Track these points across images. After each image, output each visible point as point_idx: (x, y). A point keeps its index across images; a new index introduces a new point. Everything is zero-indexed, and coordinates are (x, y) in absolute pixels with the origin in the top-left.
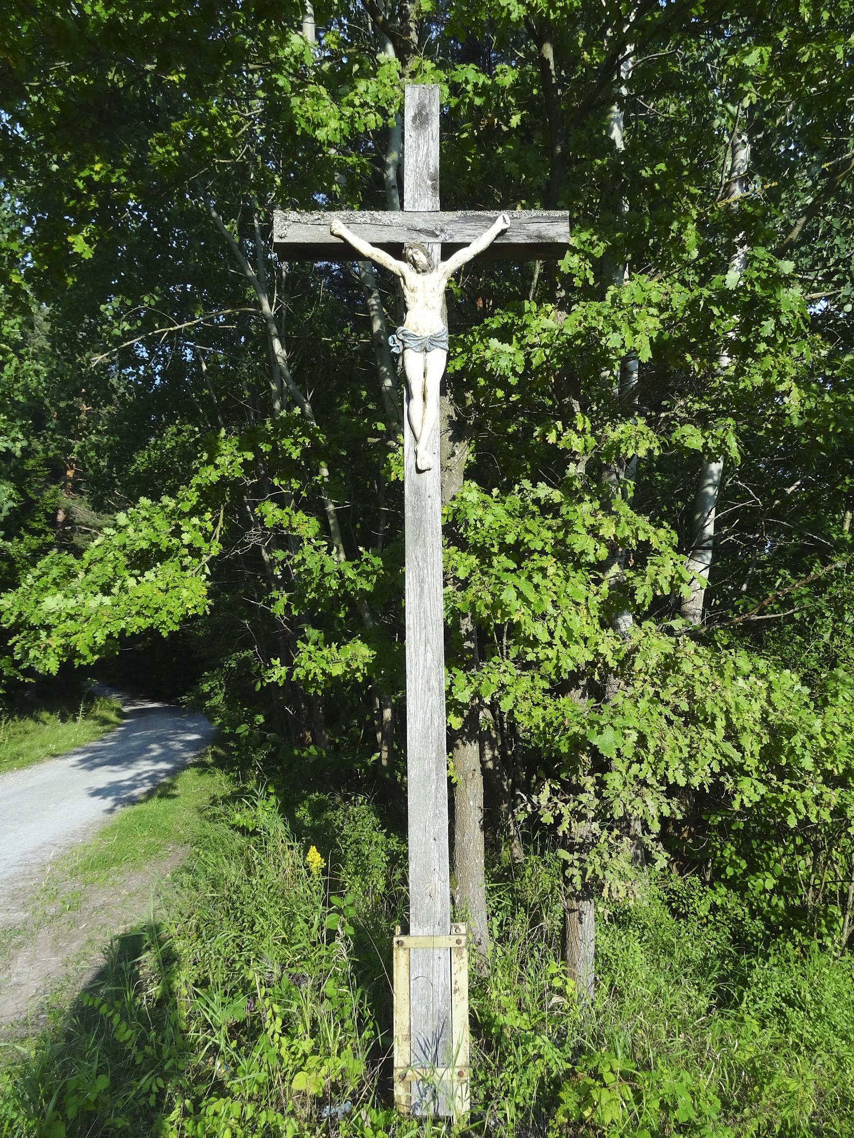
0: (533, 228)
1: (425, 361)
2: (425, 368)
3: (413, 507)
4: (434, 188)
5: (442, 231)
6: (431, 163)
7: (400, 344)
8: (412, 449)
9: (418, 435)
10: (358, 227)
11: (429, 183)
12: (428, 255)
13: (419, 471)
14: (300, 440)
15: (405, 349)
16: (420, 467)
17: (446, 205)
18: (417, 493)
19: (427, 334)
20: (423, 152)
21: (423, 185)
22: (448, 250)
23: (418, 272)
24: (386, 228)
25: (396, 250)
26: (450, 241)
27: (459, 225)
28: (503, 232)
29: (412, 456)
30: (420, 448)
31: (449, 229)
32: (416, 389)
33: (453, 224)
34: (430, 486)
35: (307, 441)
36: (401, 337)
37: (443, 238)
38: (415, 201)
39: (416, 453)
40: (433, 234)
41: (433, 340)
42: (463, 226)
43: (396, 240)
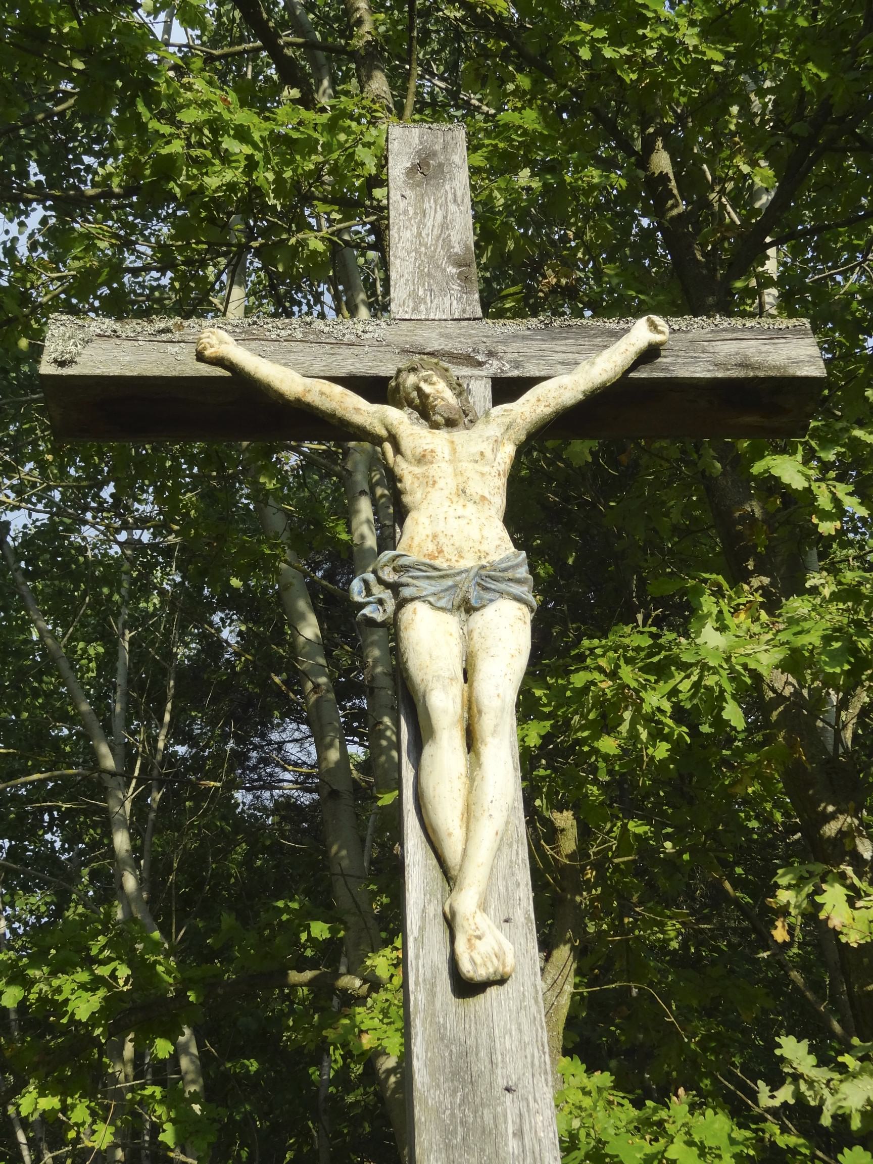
0: (727, 349)
1: (467, 636)
2: (471, 654)
3: (448, 1133)
4: (465, 279)
5: (491, 354)
6: (455, 237)
7: (387, 595)
8: (434, 910)
9: (453, 848)
10: (271, 347)
11: (453, 270)
12: (459, 389)
13: (466, 987)
14: (103, 971)
15: (401, 603)
16: (466, 967)
17: (491, 305)
18: (461, 1073)
19: (469, 562)
20: (434, 219)
21: (439, 275)
22: (507, 389)
23: (435, 426)
24: (343, 350)
25: (375, 389)
26: (515, 373)
27: (536, 345)
28: (650, 354)
29: (437, 933)
30: (467, 902)
31: (513, 350)
32: (444, 704)
33: (516, 343)
34: (507, 1043)
35: (123, 972)
36: (389, 576)
37: (493, 367)
38: (418, 301)
39: (450, 922)
40: (469, 360)
41: (489, 581)
42: (545, 346)
43: (372, 372)
